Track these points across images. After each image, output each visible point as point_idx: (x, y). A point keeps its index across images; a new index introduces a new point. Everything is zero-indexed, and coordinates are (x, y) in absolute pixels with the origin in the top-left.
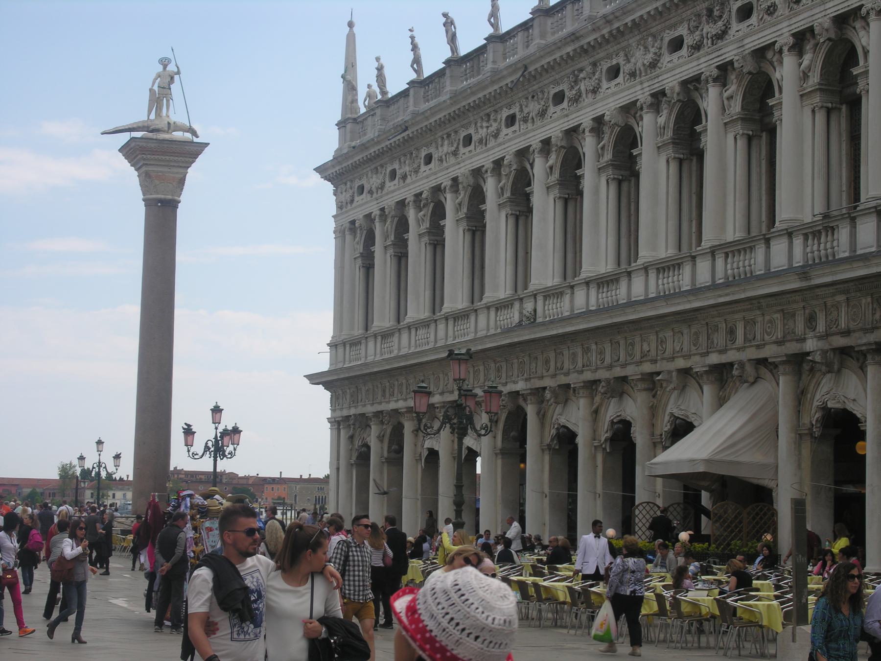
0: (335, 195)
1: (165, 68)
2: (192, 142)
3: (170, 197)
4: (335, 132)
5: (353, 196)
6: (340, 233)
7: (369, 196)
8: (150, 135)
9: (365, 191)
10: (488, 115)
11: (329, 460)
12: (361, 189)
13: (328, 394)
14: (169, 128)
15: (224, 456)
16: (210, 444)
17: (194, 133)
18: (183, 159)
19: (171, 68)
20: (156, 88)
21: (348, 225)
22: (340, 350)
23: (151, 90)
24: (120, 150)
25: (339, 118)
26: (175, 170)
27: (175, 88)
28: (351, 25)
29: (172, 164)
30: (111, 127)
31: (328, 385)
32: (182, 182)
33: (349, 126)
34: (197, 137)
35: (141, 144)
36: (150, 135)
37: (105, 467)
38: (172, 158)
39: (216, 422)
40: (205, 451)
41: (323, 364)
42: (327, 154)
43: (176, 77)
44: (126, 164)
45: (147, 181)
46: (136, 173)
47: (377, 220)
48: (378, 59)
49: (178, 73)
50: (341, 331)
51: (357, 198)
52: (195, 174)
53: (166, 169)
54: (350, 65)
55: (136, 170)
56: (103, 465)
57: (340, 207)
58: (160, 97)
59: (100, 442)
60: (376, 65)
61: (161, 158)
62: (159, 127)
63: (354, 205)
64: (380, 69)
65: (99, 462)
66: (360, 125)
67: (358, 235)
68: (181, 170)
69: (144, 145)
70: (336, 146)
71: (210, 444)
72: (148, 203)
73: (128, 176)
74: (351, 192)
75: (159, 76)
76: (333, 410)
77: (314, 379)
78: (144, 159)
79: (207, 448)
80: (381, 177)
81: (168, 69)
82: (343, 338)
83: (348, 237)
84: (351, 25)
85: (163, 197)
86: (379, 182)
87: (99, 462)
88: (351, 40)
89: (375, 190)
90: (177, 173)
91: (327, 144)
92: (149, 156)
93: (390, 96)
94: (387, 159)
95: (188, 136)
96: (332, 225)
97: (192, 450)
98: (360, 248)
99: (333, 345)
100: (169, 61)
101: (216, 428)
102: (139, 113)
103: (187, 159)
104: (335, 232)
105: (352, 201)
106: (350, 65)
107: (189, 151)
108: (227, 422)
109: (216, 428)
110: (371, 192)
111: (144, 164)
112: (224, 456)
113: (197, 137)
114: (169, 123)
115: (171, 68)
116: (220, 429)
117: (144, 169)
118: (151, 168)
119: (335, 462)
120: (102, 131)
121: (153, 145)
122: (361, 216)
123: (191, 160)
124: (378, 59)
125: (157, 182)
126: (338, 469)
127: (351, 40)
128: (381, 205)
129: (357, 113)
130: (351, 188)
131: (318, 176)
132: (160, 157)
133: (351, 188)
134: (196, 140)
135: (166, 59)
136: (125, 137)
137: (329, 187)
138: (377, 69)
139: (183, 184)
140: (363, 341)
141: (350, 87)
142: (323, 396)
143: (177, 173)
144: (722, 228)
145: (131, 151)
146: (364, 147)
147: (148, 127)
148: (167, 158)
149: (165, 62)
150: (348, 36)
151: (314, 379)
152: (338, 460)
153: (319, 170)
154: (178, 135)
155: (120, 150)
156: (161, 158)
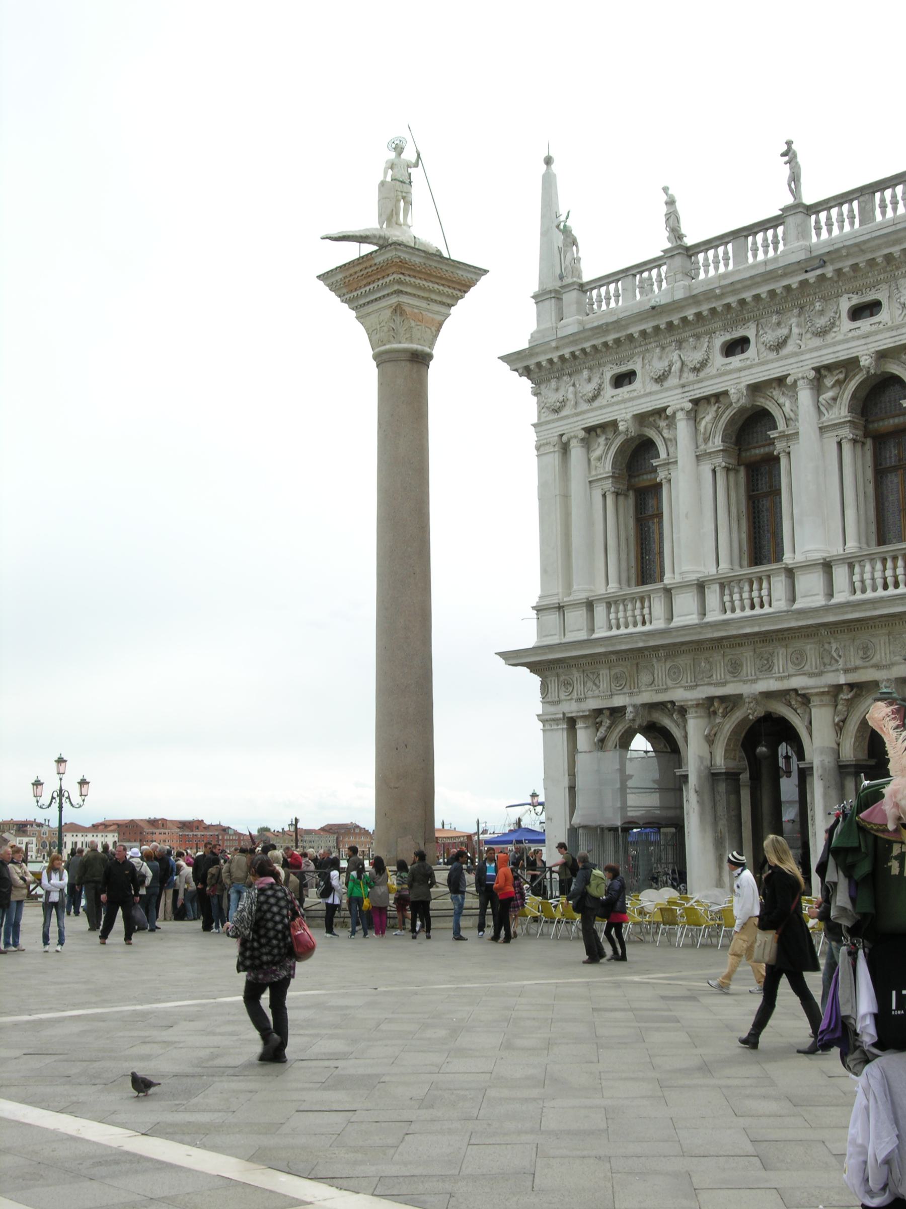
0: (536, 394)
13: (536, 680)
18: (450, 291)
19: (409, 155)
28: (548, 161)
29: (433, 297)
30: (335, 231)
31: (534, 667)
35: (403, 256)
37: (68, 798)
38: (436, 286)
41: (527, 636)
48: (665, 190)
53: (424, 304)
56: (66, 795)
59: (61, 761)
60: (664, 198)
63: (596, 404)
64: (671, 203)
65: (61, 790)
69: (407, 257)
70: (532, 326)
72: (381, 359)
77: (512, 658)
78: (400, 282)
81: (403, 156)
83: (577, 452)
84: (548, 161)
85: (419, 347)
87: (61, 790)
92: (408, 279)
96: (532, 437)
103: (455, 292)
118: (404, 299)
120: (324, 234)
123: (459, 294)
124: (665, 190)
125: (413, 324)
138: (666, 203)
148: (431, 285)
151: (512, 658)
153: (509, 359)
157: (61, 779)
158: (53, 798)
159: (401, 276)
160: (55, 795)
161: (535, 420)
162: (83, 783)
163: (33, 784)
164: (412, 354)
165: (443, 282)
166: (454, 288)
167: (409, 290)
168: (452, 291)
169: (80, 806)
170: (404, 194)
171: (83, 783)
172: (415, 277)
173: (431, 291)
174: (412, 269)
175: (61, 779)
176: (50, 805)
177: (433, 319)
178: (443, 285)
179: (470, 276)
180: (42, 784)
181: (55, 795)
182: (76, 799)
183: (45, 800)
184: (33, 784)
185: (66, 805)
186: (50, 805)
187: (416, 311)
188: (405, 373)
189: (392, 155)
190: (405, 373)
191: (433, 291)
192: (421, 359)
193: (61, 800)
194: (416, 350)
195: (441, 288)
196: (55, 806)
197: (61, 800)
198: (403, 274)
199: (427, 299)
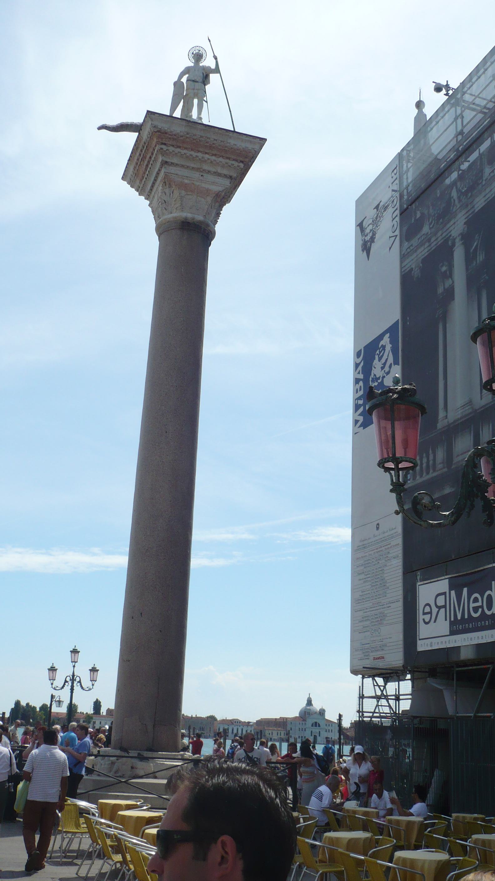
3: (200, 218)
20: (184, 80)
26: (211, 178)
29: (206, 167)
30: (114, 122)
37: (80, 682)
49: (217, 70)
56: (78, 679)
59: (75, 652)
65: (73, 675)
75: (187, 70)
85: (189, 215)
87: (73, 675)
90: (213, 183)
92: (171, 149)
111: (164, 163)
115: (208, 62)
118: (172, 170)
132: (189, 153)
149: (198, 57)
157: (74, 666)
158: (66, 681)
159: (163, 146)
160: (68, 679)
162: (94, 670)
163: (49, 670)
164: (183, 222)
165: (215, 152)
166: (227, 158)
167: (175, 160)
168: (228, 161)
169: (90, 690)
170: (196, 91)
171: (94, 670)
172: (179, 147)
173: (202, 161)
174: (174, 139)
175: (74, 666)
176: (63, 687)
177: (208, 190)
178: (213, 155)
179: (250, 146)
180: (56, 670)
181: (68, 679)
182: (86, 683)
183: (59, 682)
184: (49, 670)
185: (77, 688)
186: (63, 687)
187: (186, 181)
188: (186, 247)
190: (186, 247)
191: (205, 161)
192: (207, 235)
193: (73, 683)
194: (186, 218)
195: (213, 158)
196: (68, 688)
197: (73, 683)
198: (165, 144)
199: (198, 170)
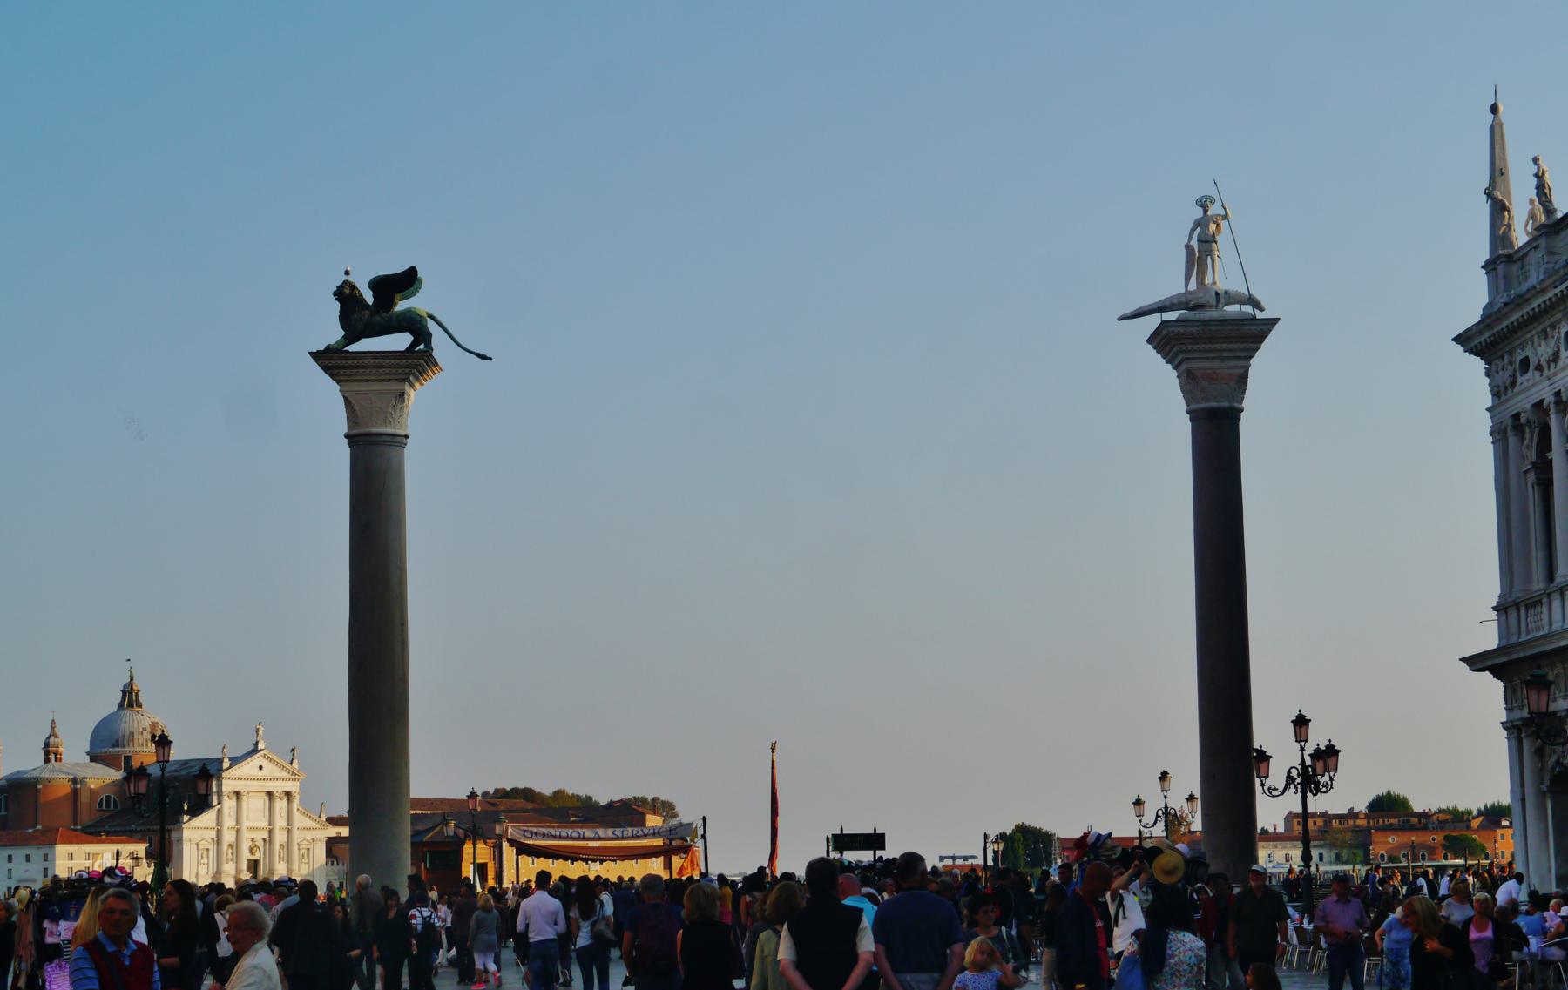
0: (1488, 375)
1: (1205, 211)
2: (1254, 318)
3: (1226, 404)
4: (1482, 280)
5: (1514, 377)
6: (1499, 434)
7: (1537, 374)
8: (1190, 315)
9: (1532, 367)
10: (1545, 331)
11: (1509, 787)
12: (1525, 363)
13: (1499, 686)
14: (1218, 301)
15: (1318, 791)
16: (1294, 773)
17: (1256, 305)
19: (1214, 210)
20: (1194, 243)
21: (1509, 422)
22: (1513, 615)
23: (1188, 248)
24: (1149, 341)
25: (1486, 256)
27: (1223, 244)
28: (1494, 109)
31: (1497, 672)
32: (1242, 380)
33: (1501, 268)
34: (1262, 310)
36: (1190, 315)
39: (1301, 738)
40: (1287, 784)
41: (1488, 638)
42: (1471, 316)
43: (1224, 224)
44: (1159, 359)
45: (1191, 384)
46: (1175, 373)
47: (1552, 410)
48: (1535, 160)
49: (1226, 217)
50: (1511, 587)
51: (1520, 379)
52: (1262, 365)
53: (1217, 363)
54: (1497, 172)
55: (1175, 368)
57: (1497, 393)
58: (1200, 254)
61: (1210, 346)
62: (1203, 301)
63: (1516, 390)
64: (1540, 177)
66: (1519, 265)
67: (1527, 435)
68: (1241, 363)
69: (1181, 330)
70: (1485, 300)
71: (1294, 773)
72: (1195, 416)
73: (1163, 381)
74: (1511, 369)
76: (1509, 709)
77: (1476, 662)
79: (1290, 779)
80: (1552, 343)
82: (1515, 595)
83: (1512, 440)
84: (1494, 109)
85: (1215, 404)
86: (1550, 351)
88: (1495, 132)
89: (1545, 365)
91: (1471, 299)
93: (1559, 215)
94: (1559, 316)
95: (1248, 309)
96: (1486, 423)
97: (1268, 783)
98: (1532, 455)
99: (1500, 609)
100: (1213, 201)
101: (1302, 749)
102: (1171, 282)
104: (1491, 434)
105: (1513, 384)
106: (1497, 172)
107: (1250, 333)
108: (1318, 738)
109: (1302, 749)
110: (1539, 368)
112: (1318, 791)
113: (1262, 310)
114: (1217, 294)
116: (1310, 748)
117: (1184, 366)
119: (1518, 790)
121: (1194, 329)
122: (1528, 406)
124: (1535, 160)
125: (1205, 384)
126: (1523, 801)
127: (1495, 132)
128: (1556, 387)
129: (1512, 245)
130: (1511, 363)
131: (1459, 348)
133: (1511, 363)
134: (1259, 315)
135: (1207, 197)
136: (1153, 321)
137: (1479, 364)
138: (1536, 175)
139: (1245, 383)
140: (1545, 600)
141: (1499, 209)
142: (1491, 688)
143: (1235, 367)
144: (1528, 580)
145: (1163, 341)
146: (1521, 300)
147: (1187, 303)
148: (1218, 346)
149: (1204, 203)
150: (1492, 128)
151: (1476, 662)
152: (1522, 786)
154: (1233, 309)
155: (1149, 341)
156: (1210, 346)
161: (1489, 403)
189: (1199, 213)
